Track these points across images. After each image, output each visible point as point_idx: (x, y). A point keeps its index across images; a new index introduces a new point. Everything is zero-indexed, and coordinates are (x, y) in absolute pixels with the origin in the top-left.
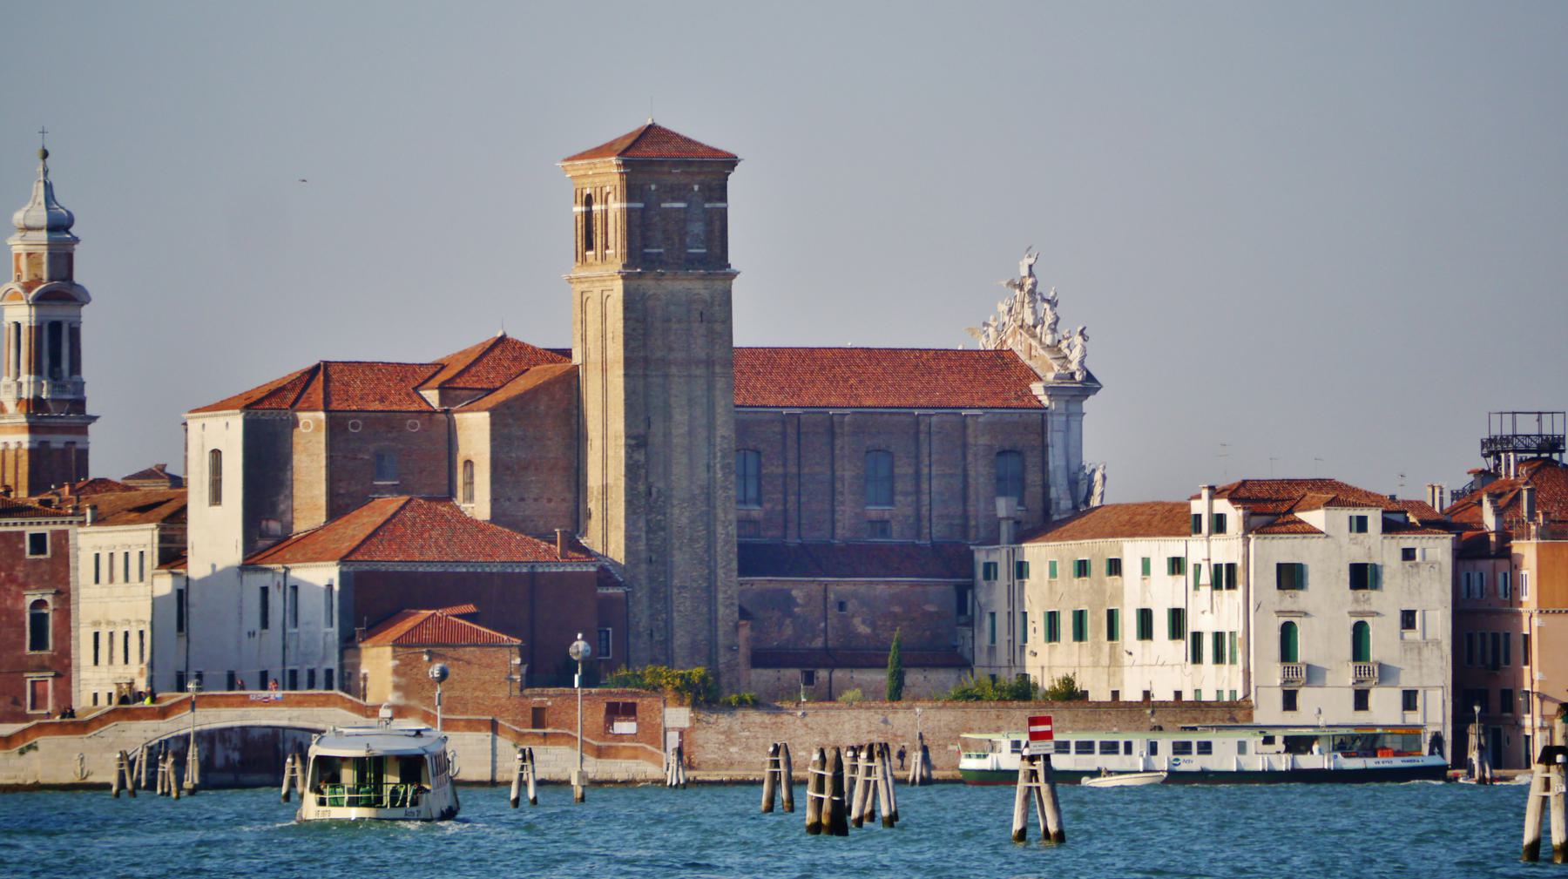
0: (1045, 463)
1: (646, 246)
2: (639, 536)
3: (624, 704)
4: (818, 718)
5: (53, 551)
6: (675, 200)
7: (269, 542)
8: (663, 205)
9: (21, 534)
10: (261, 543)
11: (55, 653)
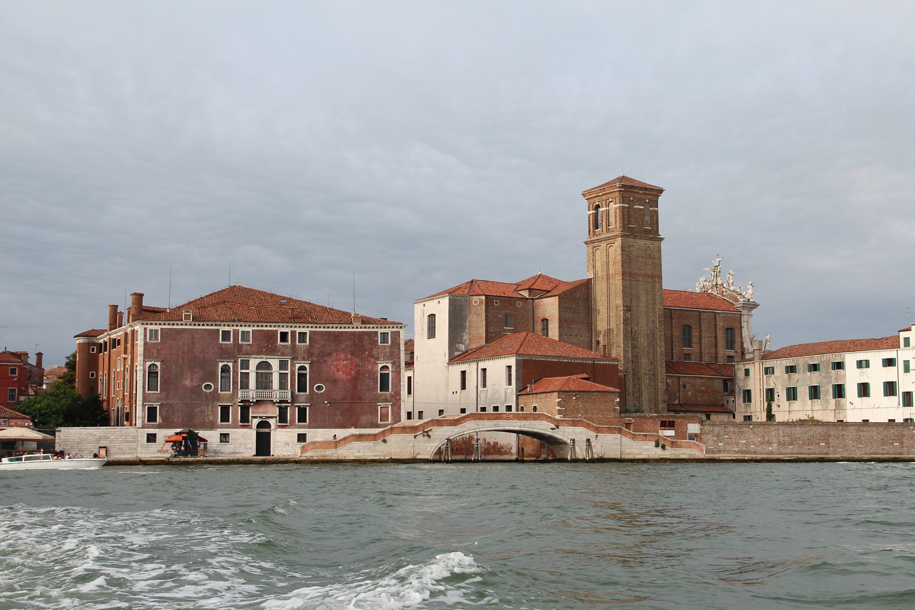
0: (741, 334)
1: (629, 224)
2: (629, 350)
3: (669, 421)
4: (760, 429)
5: (392, 342)
6: (640, 205)
7: (460, 353)
9: (376, 333)
10: (456, 354)
11: (393, 393)
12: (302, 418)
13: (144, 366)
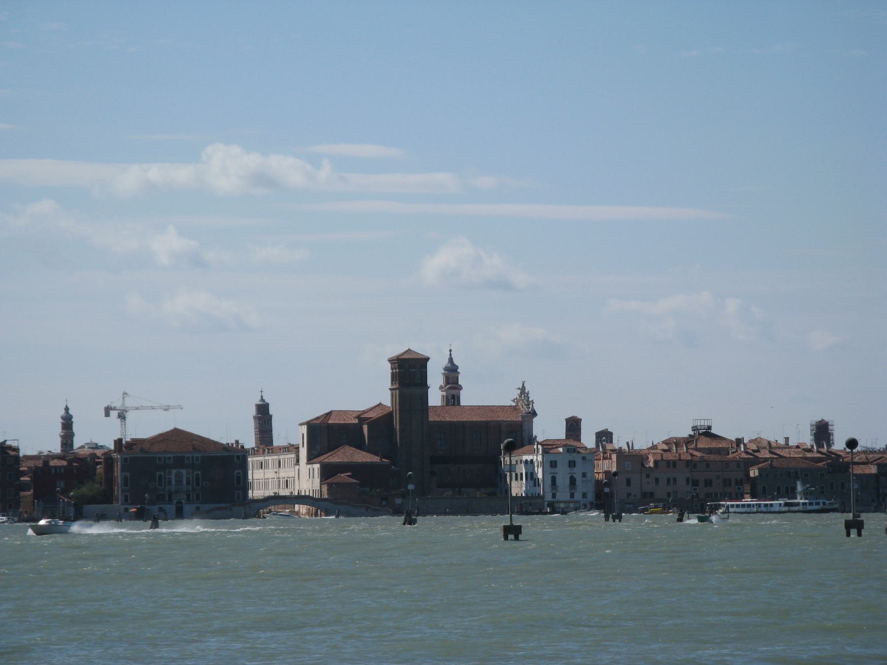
8: (411, 370)
12: (198, 499)
13: (122, 475)
